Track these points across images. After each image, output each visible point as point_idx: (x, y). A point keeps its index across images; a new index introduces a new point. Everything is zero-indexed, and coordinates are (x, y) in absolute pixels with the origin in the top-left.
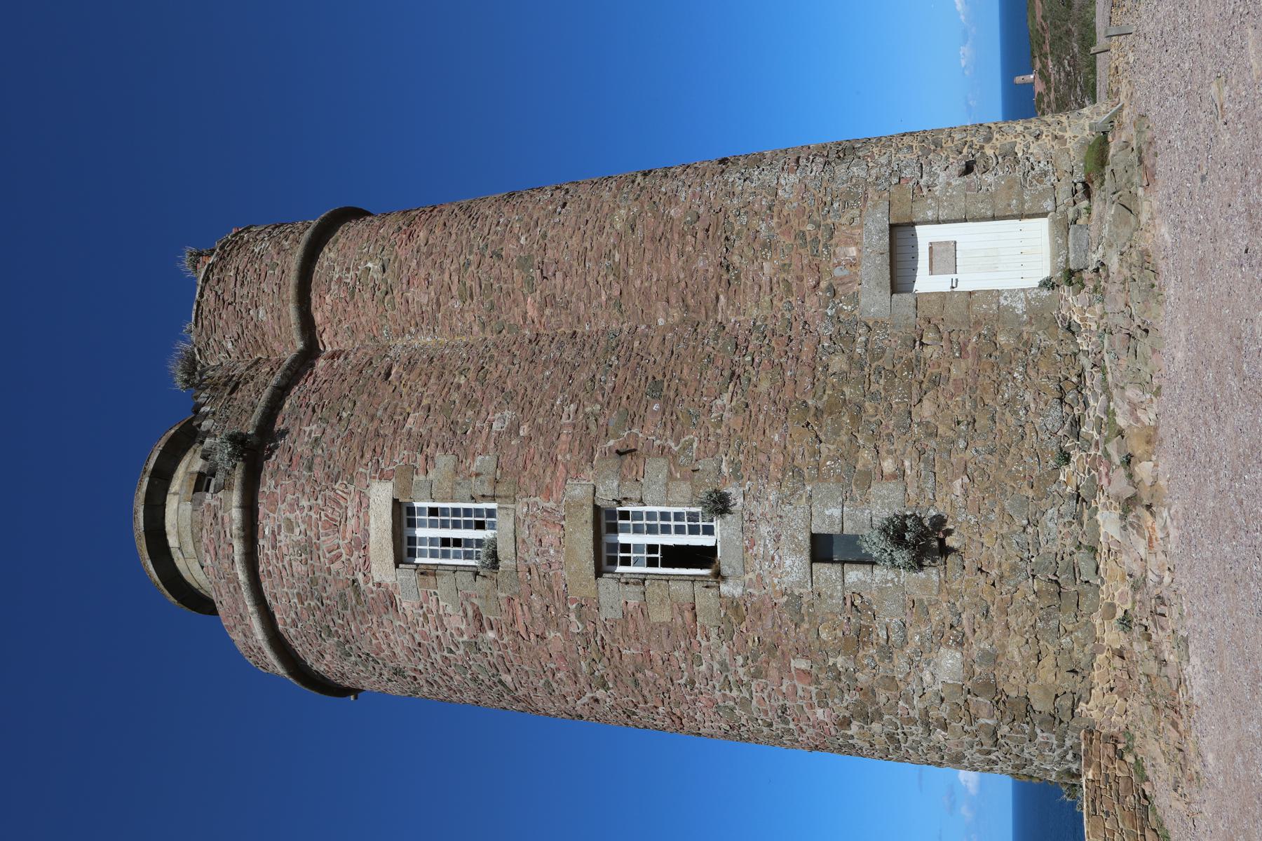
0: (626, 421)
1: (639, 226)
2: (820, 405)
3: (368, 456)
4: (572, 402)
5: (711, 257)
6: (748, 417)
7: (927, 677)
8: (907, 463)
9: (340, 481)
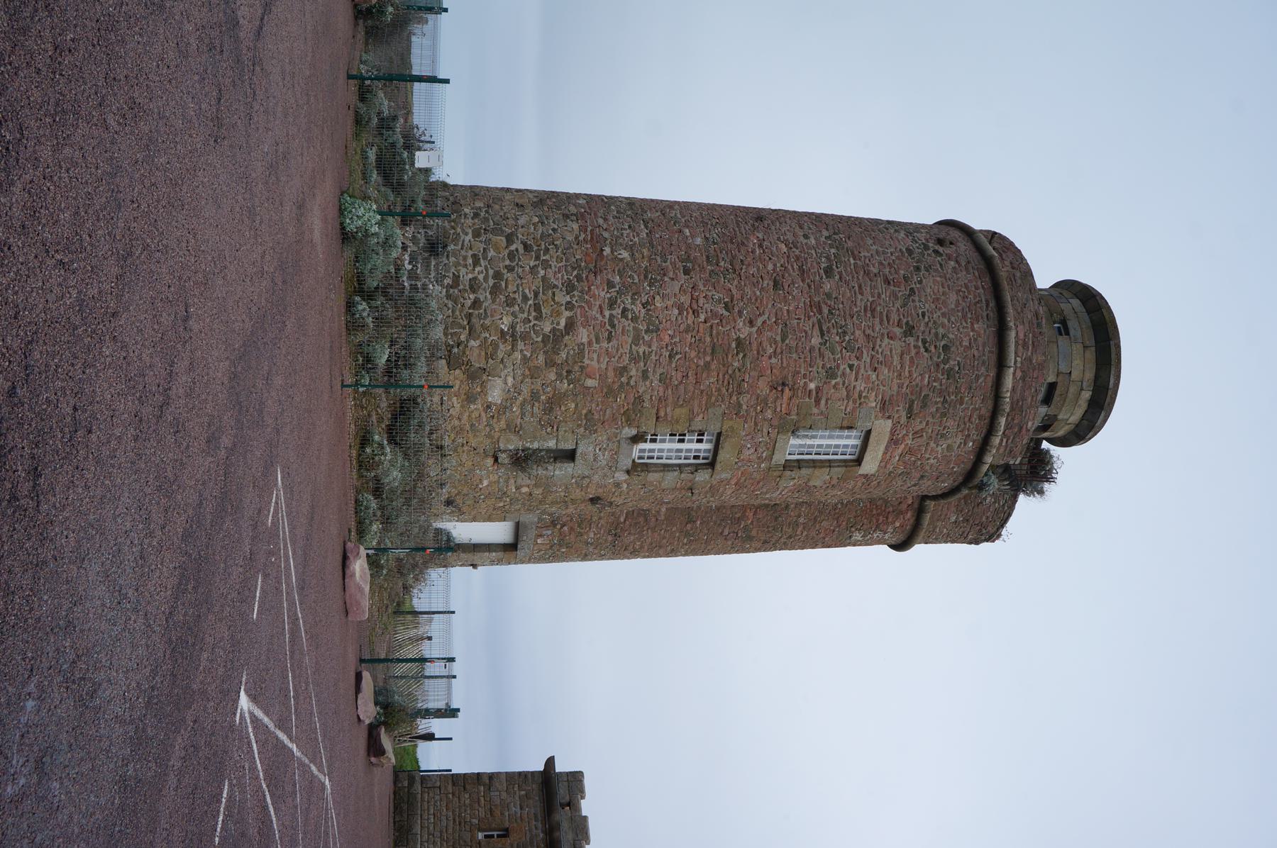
7: (510, 380)
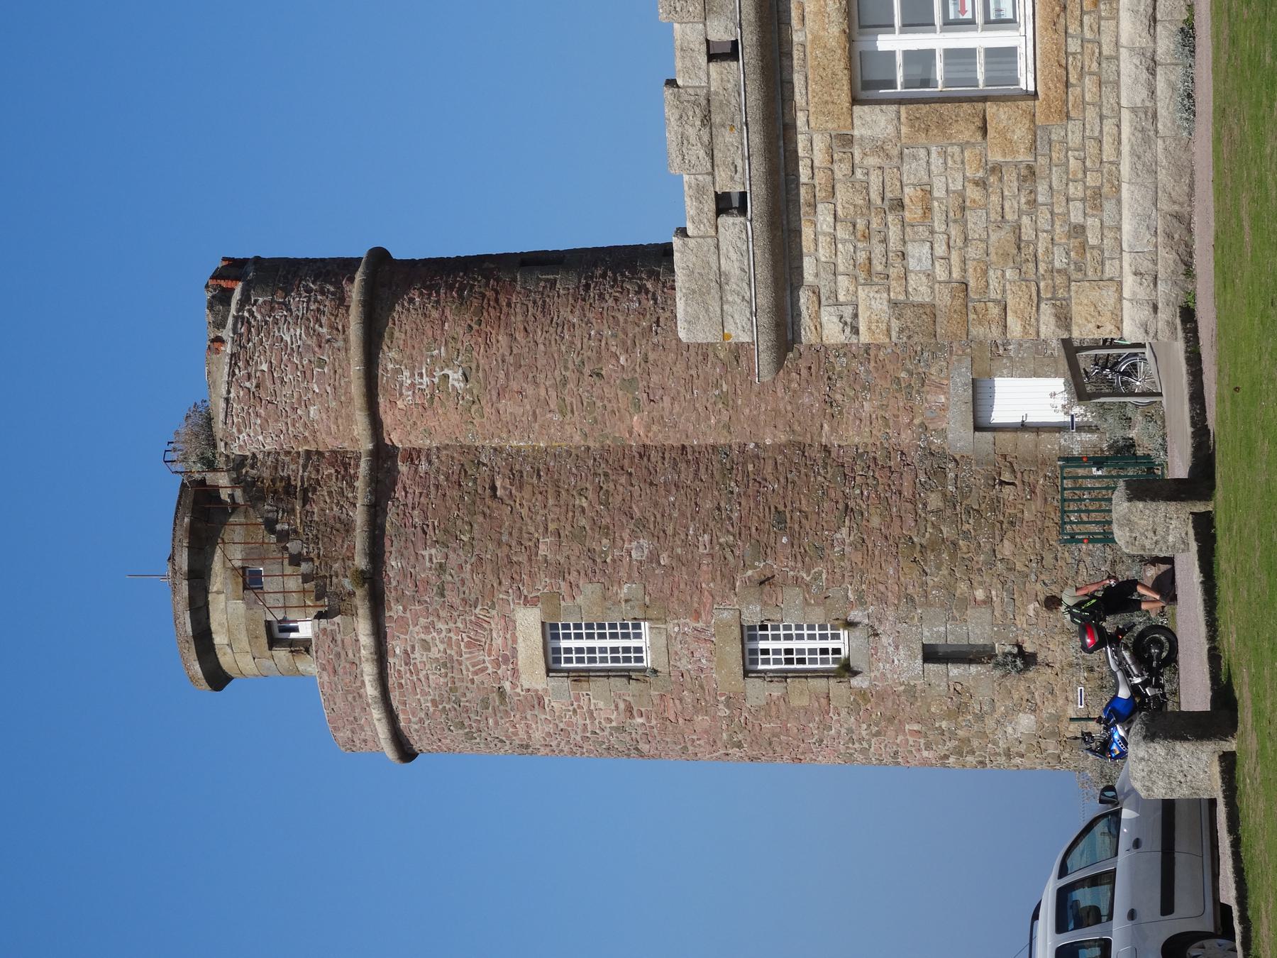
0: (759, 552)
2: (924, 542)
3: (506, 582)
4: (704, 532)
5: (816, 394)
6: (866, 552)
7: (1010, 730)
8: (994, 593)
9: (479, 607)
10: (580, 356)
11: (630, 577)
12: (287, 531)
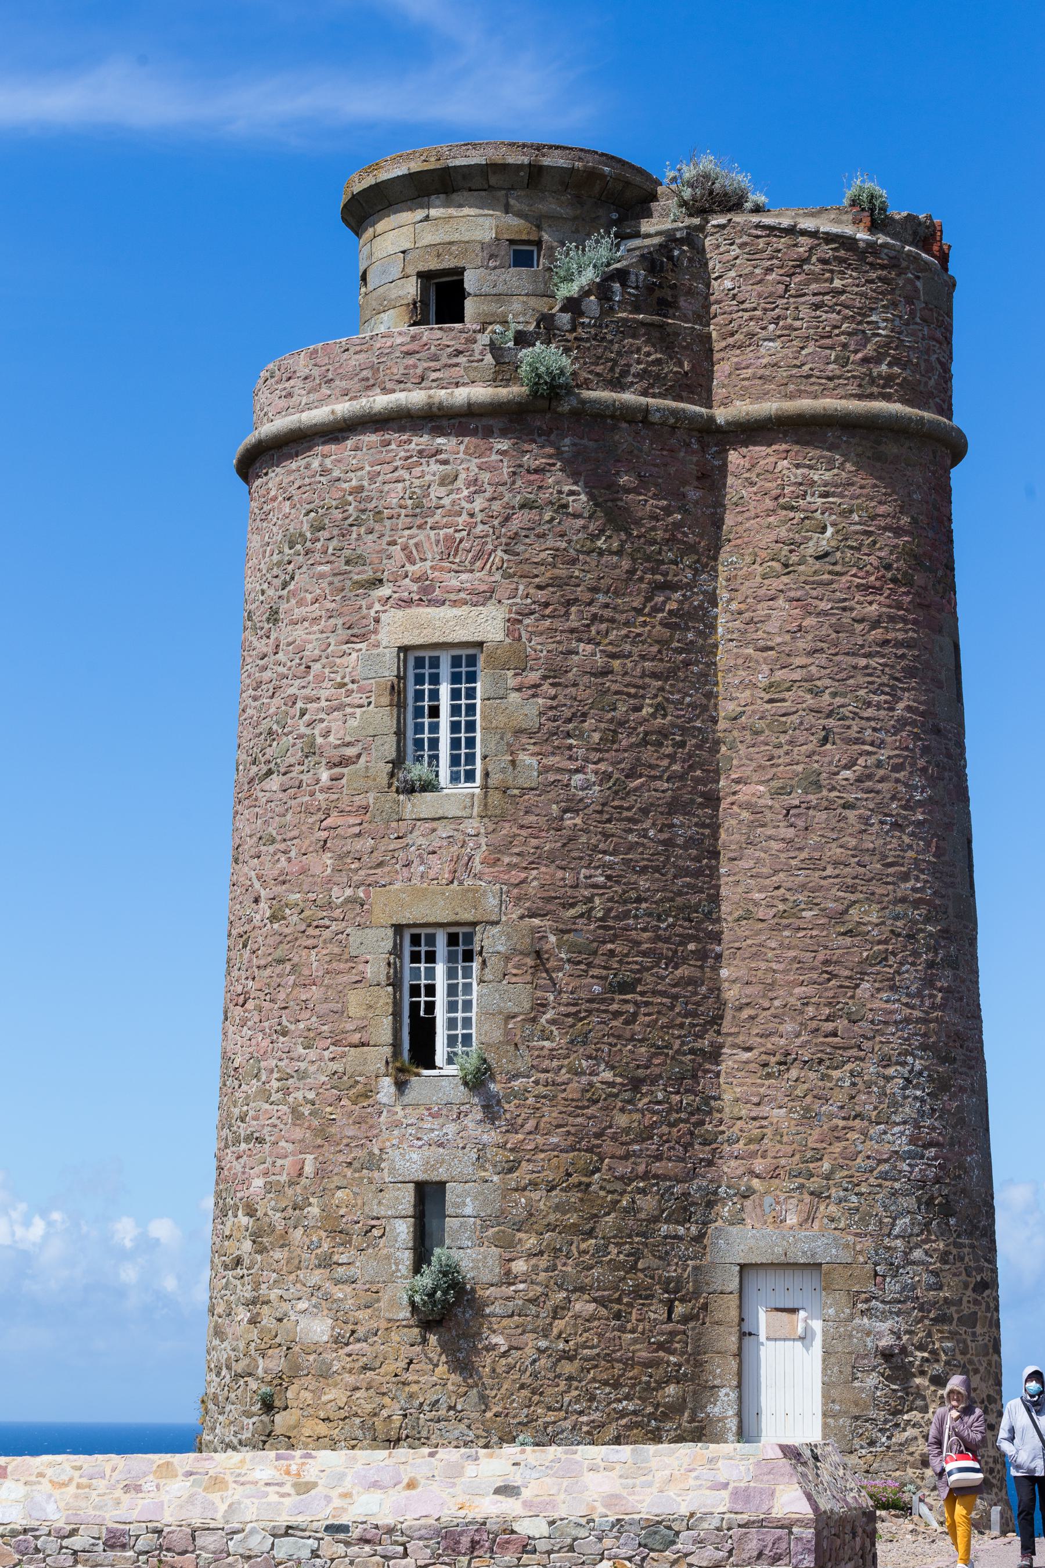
1: (848, 940)
2: (593, 1188)
3: (541, 595)
4: (609, 878)
5: (799, 1041)
7: (302, 1305)
8: (522, 1286)
9: (506, 557)
10: (851, 715)
11: (545, 770)
12: (610, 299)
